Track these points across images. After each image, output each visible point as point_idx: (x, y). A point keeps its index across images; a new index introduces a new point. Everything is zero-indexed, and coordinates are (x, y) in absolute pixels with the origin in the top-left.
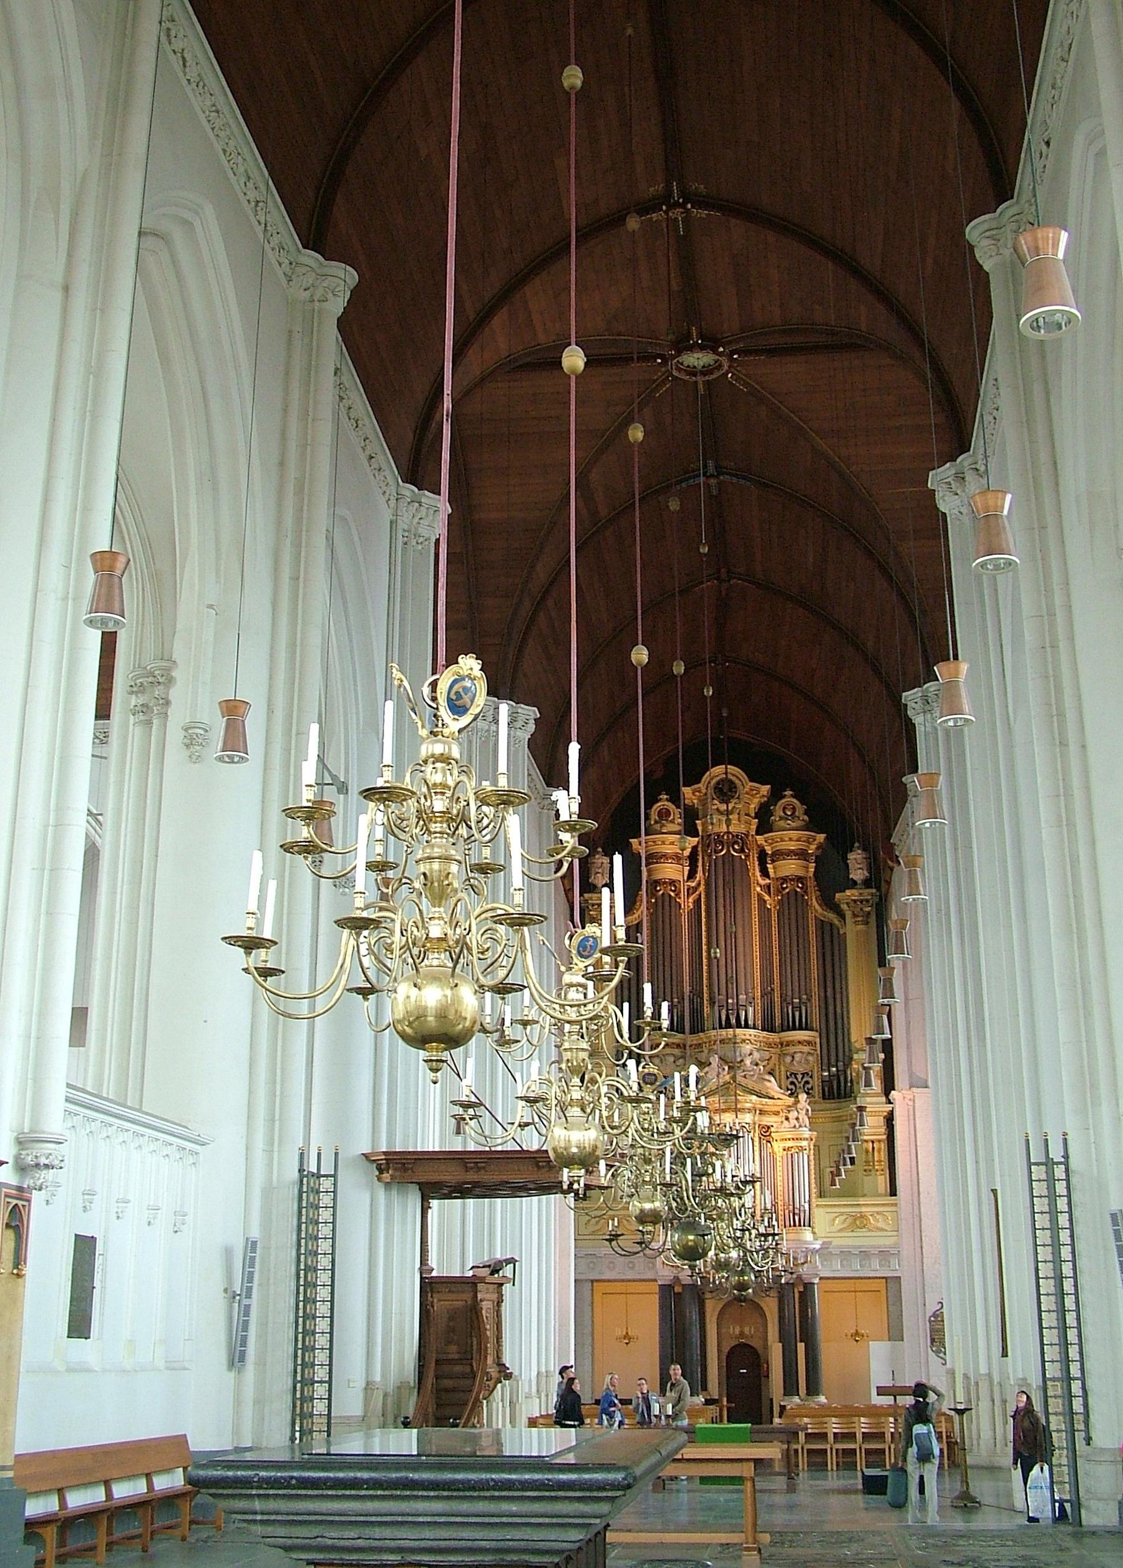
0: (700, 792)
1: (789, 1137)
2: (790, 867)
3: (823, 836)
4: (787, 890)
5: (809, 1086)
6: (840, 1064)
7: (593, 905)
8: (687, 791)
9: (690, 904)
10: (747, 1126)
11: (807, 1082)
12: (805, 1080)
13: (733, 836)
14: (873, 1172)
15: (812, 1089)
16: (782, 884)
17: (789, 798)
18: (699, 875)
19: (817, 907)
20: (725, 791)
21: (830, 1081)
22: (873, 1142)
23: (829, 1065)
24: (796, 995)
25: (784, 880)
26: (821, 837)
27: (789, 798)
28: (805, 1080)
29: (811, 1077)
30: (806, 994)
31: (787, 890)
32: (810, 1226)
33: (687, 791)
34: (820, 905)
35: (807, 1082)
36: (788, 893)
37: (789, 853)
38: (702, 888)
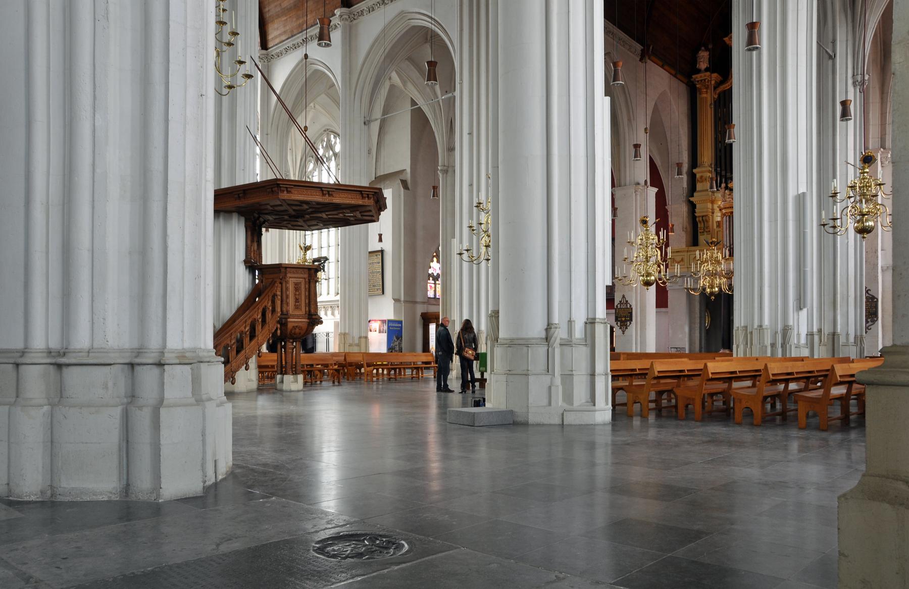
7: (698, 81)
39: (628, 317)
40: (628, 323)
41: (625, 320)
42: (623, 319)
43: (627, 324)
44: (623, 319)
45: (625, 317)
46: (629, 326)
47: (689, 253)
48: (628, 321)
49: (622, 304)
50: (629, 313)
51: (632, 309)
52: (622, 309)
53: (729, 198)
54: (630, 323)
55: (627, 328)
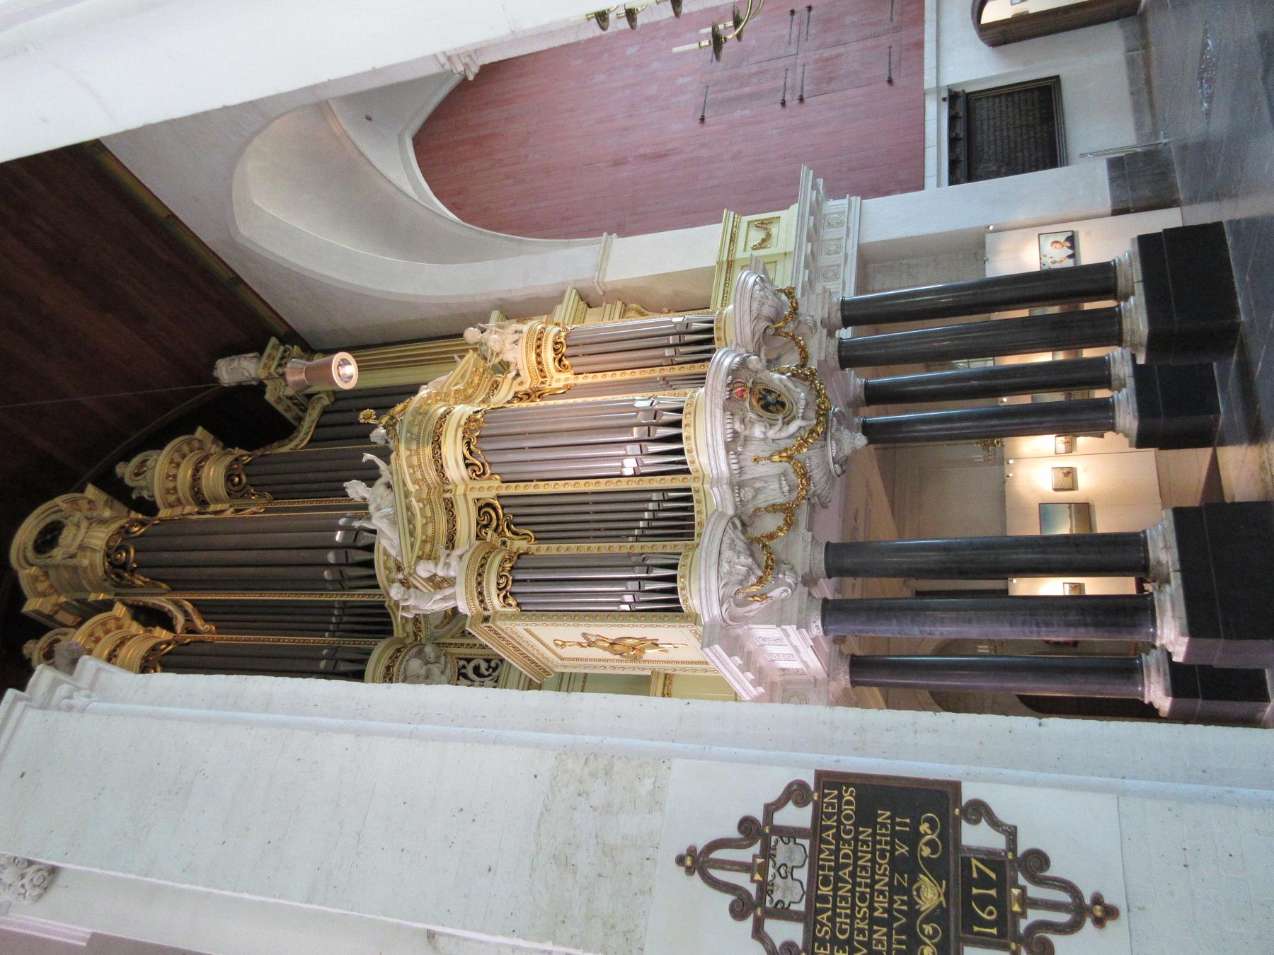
0: (35, 579)
1: (534, 356)
2: (214, 475)
3: (200, 429)
4: (244, 477)
8: (32, 605)
9: (207, 626)
13: (118, 533)
16: (232, 481)
17: (125, 471)
18: (163, 602)
19: (292, 445)
20: (48, 538)
25: (229, 478)
26: (200, 432)
27: (125, 471)
31: (244, 477)
33: (32, 605)
34: (292, 440)
36: (247, 476)
37: (197, 470)
38: (185, 599)
39: (913, 838)
40: (976, 836)
41: (938, 870)
42: (930, 895)
43: (991, 859)
44: (930, 895)
45: (908, 867)
46: (1011, 834)
48: (949, 834)
49: (765, 888)
50: (865, 817)
51: (828, 780)
52: (813, 897)
53: (447, 565)
54: (979, 811)
55: (1036, 862)
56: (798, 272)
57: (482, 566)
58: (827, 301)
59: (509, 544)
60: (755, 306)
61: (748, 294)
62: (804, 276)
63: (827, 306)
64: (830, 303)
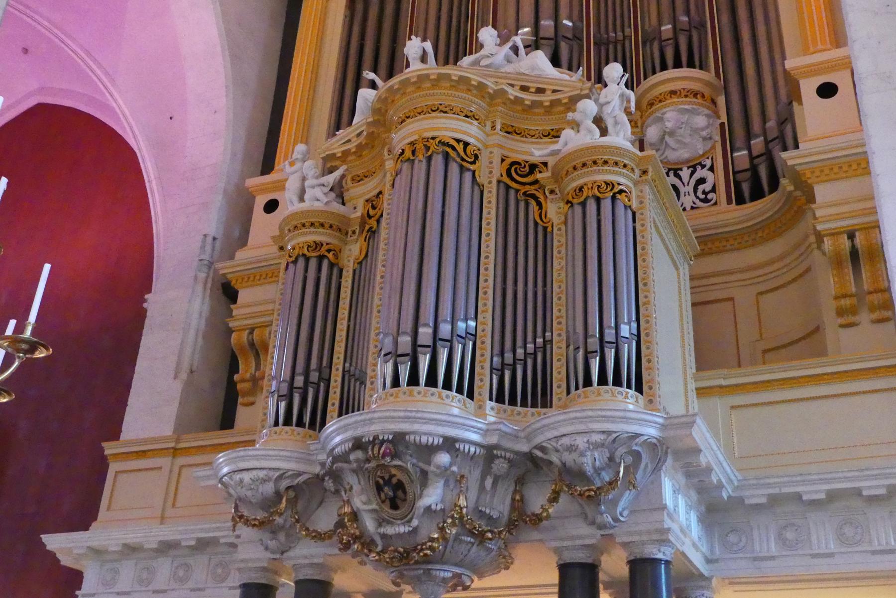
5: (707, 187)
6: (771, 124)
10: (460, 148)
11: (702, 181)
12: (697, 176)
14: (864, 317)
15: (714, 190)
21: (754, 169)
22: (851, 236)
23: (749, 136)
24: (666, 15)
28: (697, 176)
29: (712, 169)
30: (688, 12)
32: (639, 389)
35: (702, 181)
47: (181, 461)
56: (876, 477)
57: (304, 225)
58: (645, 538)
59: (355, 237)
60: (566, 441)
61: (581, 427)
62: (870, 487)
63: (636, 538)
64: (643, 543)
